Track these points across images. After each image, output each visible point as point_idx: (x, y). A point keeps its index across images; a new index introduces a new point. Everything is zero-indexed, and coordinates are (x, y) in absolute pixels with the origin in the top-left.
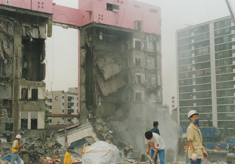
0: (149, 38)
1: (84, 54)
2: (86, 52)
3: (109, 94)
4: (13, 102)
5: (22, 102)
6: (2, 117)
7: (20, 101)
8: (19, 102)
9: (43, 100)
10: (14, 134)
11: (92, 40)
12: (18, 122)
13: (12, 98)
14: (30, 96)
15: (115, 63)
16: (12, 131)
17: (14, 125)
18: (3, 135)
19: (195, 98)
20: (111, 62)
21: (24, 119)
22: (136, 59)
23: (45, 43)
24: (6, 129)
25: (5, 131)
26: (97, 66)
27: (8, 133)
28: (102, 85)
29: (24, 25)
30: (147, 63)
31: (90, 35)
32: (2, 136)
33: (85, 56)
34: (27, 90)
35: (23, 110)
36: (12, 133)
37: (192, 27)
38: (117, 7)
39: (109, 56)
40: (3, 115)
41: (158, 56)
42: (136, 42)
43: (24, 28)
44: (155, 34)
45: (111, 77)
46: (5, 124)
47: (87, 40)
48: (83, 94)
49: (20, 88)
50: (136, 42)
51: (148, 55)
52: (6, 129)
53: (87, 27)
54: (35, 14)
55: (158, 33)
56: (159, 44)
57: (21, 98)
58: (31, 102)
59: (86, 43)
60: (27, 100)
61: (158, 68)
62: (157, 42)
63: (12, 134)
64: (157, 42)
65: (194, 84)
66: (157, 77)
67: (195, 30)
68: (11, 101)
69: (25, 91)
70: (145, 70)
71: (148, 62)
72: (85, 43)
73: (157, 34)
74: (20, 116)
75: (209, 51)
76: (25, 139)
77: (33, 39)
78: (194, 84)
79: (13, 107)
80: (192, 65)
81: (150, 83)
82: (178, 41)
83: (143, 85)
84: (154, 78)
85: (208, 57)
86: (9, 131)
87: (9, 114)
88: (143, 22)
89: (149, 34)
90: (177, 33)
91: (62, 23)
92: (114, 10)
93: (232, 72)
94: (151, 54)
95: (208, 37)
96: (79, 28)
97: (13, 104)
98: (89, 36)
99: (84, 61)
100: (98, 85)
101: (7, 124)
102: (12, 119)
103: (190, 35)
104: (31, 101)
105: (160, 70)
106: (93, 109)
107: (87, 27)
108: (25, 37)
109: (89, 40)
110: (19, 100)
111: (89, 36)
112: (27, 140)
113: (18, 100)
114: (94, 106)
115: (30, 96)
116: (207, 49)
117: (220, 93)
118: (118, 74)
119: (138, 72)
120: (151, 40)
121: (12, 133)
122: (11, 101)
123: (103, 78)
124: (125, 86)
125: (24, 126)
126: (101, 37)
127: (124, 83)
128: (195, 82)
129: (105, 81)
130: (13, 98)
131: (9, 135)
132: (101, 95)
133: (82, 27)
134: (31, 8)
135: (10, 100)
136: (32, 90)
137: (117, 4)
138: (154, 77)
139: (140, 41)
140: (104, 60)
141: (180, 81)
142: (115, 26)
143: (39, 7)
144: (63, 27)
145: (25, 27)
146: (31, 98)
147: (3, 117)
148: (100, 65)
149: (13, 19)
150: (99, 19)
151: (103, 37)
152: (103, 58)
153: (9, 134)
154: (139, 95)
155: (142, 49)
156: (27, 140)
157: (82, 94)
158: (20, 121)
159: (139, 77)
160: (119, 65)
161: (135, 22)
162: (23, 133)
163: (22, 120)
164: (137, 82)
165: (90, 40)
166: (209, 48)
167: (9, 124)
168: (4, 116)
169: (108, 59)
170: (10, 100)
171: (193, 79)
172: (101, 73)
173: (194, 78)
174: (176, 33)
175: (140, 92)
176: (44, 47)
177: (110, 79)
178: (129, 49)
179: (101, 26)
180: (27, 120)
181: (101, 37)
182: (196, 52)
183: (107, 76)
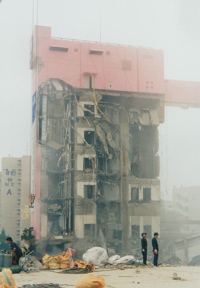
4: (122, 204)
5: (132, 205)
6: (109, 222)
7: (130, 203)
8: (129, 205)
9: (158, 202)
10: (123, 244)
12: (128, 228)
13: (120, 200)
16: (120, 239)
17: (123, 232)
18: (110, 245)
21: (135, 225)
24: (115, 237)
25: (113, 239)
27: (117, 242)
32: (110, 246)
35: (133, 214)
36: (121, 242)
40: (109, 220)
46: (113, 231)
52: (115, 237)
57: (130, 199)
58: (143, 205)
60: (138, 202)
63: (121, 244)
68: (120, 203)
74: (130, 221)
76: (136, 250)
79: (122, 210)
86: (117, 240)
87: (117, 219)
97: (122, 206)
101: (115, 231)
102: (120, 225)
104: (143, 204)
110: (129, 203)
112: (138, 251)
113: (127, 202)
121: (121, 242)
122: (120, 203)
125: (136, 233)
130: (121, 200)
131: (117, 244)
135: (118, 202)
146: (143, 199)
147: (110, 223)
149: (118, 105)
153: (117, 243)
156: (138, 251)
162: (135, 242)
167: (116, 231)
168: (111, 221)
170: (117, 203)
180: (139, 226)
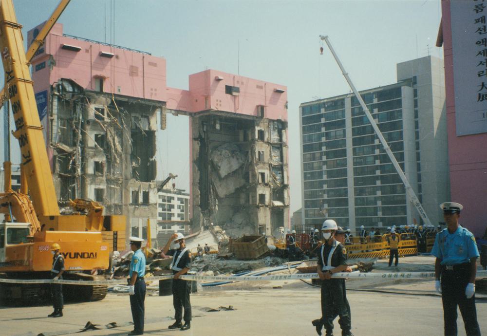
0: (274, 126)
1: (197, 147)
2: (200, 145)
3: (226, 195)
11: (207, 130)
14: (141, 200)
15: (233, 157)
19: (325, 197)
20: (228, 155)
22: (259, 152)
23: (155, 136)
26: (212, 162)
28: (217, 184)
29: (133, 115)
30: (271, 157)
31: (205, 123)
33: (199, 150)
34: (137, 193)
35: (134, 216)
37: (322, 101)
38: (237, 90)
39: (225, 148)
41: (284, 148)
42: (259, 131)
43: (133, 119)
44: (280, 120)
45: (228, 174)
47: (202, 129)
48: (197, 196)
49: (131, 190)
50: (259, 131)
51: (273, 147)
53: (201, 115)
54: (147, 103)
55: (284, 119)
56: (286, 131)
57: (131, 202)
59: (200, 134)
60: (138, 205)
61: (285, 162)
62: (283, 131)
64: (283, 131)
65: (325, 177)
66: (283, 174)
67: (326, 106)
69: (136, 193)
70: (269, 167)
71: (272, 155)
72: (198, 134)
73: (283, 120)
74: (131, 223)
75: (344, 135)
77: (146, 131)
78: (325, 177)
80: (322, 152)
81: (274, 181)
82: (303, 118)
83: (267, 185)
84: (280, 175)
85: (344, 142)
88: (266, 106)
89: (273, 121)
90: (301, 108)
91: (171, 110)
92: (234, 94)
93: (375, 163)
94: (276, 146)
95: (344, 116)
96: (191, 114)
98: (203, 125)
99: (198, 156)
100: (213, 185)
103: (320, 111)
105: (287, 165)
106: (208, 214)
107: (201, 115)
108: (133, 129)
109: (203, 129)
111: (203, 125)
114: (209, 211)
115: (141, 200)
116: (342, 133)
117: (359, 192)
118: (236, 170)
119: (262, 168)
120: (276, 128)
122: (121, 206)
123: (219, 176)
124: (244, 186)
126: (218, 127)
127: (243, 181)
128: (326, 176)
129: (220, 179)
132: (217, 196)
133: (195, 114)
134: (144, 96)
136: (143, 192)
137: (236, 85)
138: (279, 173)
139: (263, 130)
140: (219, 153)
141: (305, 175)
142: (235, 114)
143: (152, 94)
144: (173, 114)
145: (135, 117)
148: (216, 160)
150: (217, 104)
151: (221, 125)
152: (219, 151)
154: (262, 197)
155: (266, 140)
157: (195, 196)
158: (131, 230)
159: (263, 175)
160: (238, 159)
161: (258, 107)
163: (133, 228)
164: (260, 181)
165: (205, 130)
166: (344, 131)
169: (224, 152)
171: (324, 172)
172: (216, 169)
173: (325, 171)
174: (300, 107)
175: (264, 193)
176: (155, 141)
177: (227, 177)
178: (250, 139)
179: (219, 114)
180: (138, 228)
181: (218, 127)
182: (327, 135)
183: (223, 172)
